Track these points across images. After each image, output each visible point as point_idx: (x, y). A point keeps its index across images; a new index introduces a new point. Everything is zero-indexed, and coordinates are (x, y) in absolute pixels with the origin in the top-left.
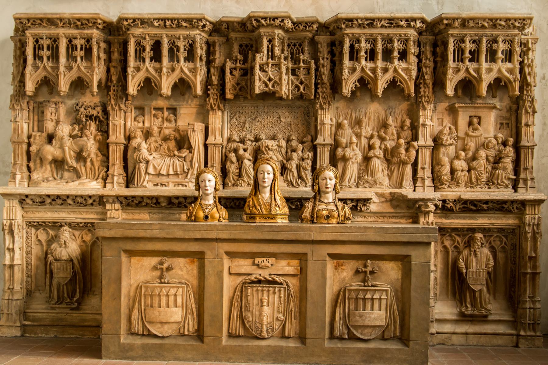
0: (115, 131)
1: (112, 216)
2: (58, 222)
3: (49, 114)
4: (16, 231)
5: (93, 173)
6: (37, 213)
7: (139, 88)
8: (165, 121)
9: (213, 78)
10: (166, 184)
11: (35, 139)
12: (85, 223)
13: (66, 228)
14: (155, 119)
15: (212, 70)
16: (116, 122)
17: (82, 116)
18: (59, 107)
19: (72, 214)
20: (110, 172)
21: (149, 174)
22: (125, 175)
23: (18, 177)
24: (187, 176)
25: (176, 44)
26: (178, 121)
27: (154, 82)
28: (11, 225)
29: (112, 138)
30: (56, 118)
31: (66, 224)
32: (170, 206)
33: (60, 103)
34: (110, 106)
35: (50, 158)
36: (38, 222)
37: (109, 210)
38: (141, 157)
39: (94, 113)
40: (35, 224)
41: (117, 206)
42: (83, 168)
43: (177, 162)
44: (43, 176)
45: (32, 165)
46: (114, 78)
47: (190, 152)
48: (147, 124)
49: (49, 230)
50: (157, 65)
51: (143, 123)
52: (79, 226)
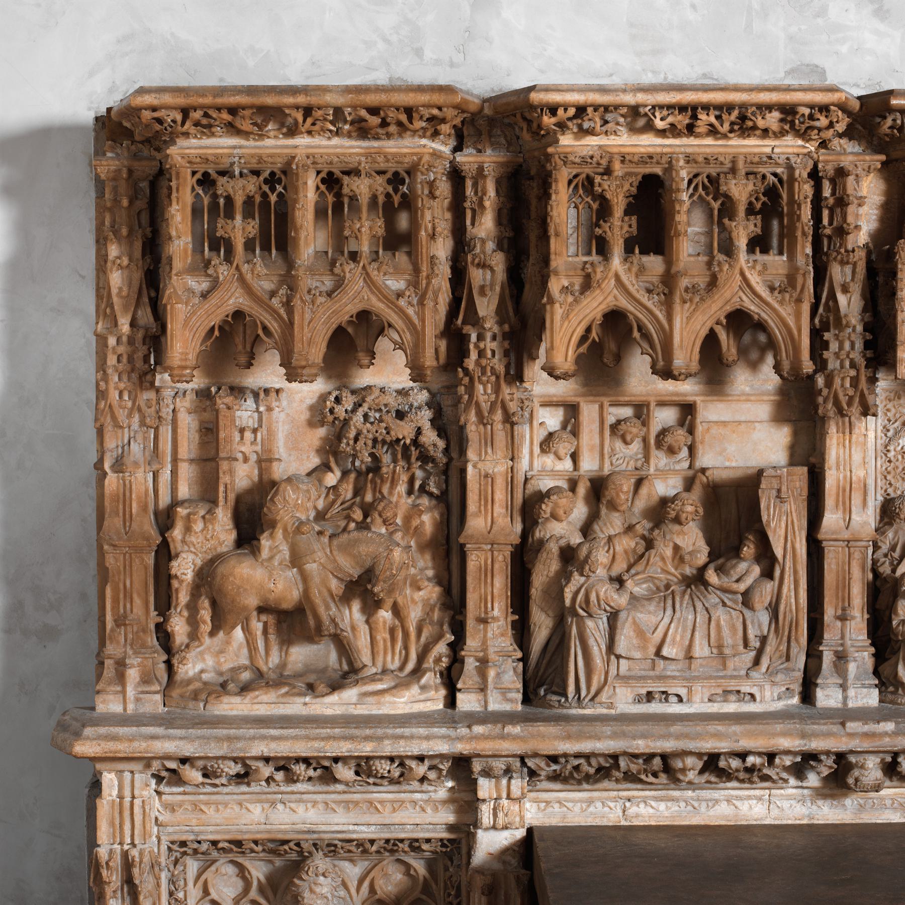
0: (487, 500)
1: (501, 821)
2: (285, 842)
3: (237, 436)
4: (144, 881)
5: (399, 644)
6: (210, 811)
7: (583, 349)
8: (654, 452)
9: (842, 299)
10: (683, 692)
11: (188, 529)
12: (387, 841)
13: (320, 862)
14: (619, 444)
15: (838, 273)
16: (488, 466)
17: (360, 444)
18: (270, 409)
19: (340, 810)
20: (472, 643)
21: (618, 657)
22: (519, 654)
23: (133, 674)
24: (757, 662)
25: (723, 188)
26: (700, 449)
27: (640, 329)
28: (128, 864)
29: (476, 523)
30: (258, 448)
31: (315, 845)
32: (706, 776)
33: (273, 394)
34: (473, 412)
35: (252, 601)
36: (214, 843)
37: (484, 800)
38: (593, 597)
39: (404, 431)
40: (204, 847)
41: (518, 785)
42: (363, 629)
43: (720, 614)
44: (218, 663)
45: (179, 627)
46: (486, 307)
47: (768, 574)
48: (589, 464)
49: (247, 863)
50: (654, 263)
51: (575, 457)
52: (365, 851)
